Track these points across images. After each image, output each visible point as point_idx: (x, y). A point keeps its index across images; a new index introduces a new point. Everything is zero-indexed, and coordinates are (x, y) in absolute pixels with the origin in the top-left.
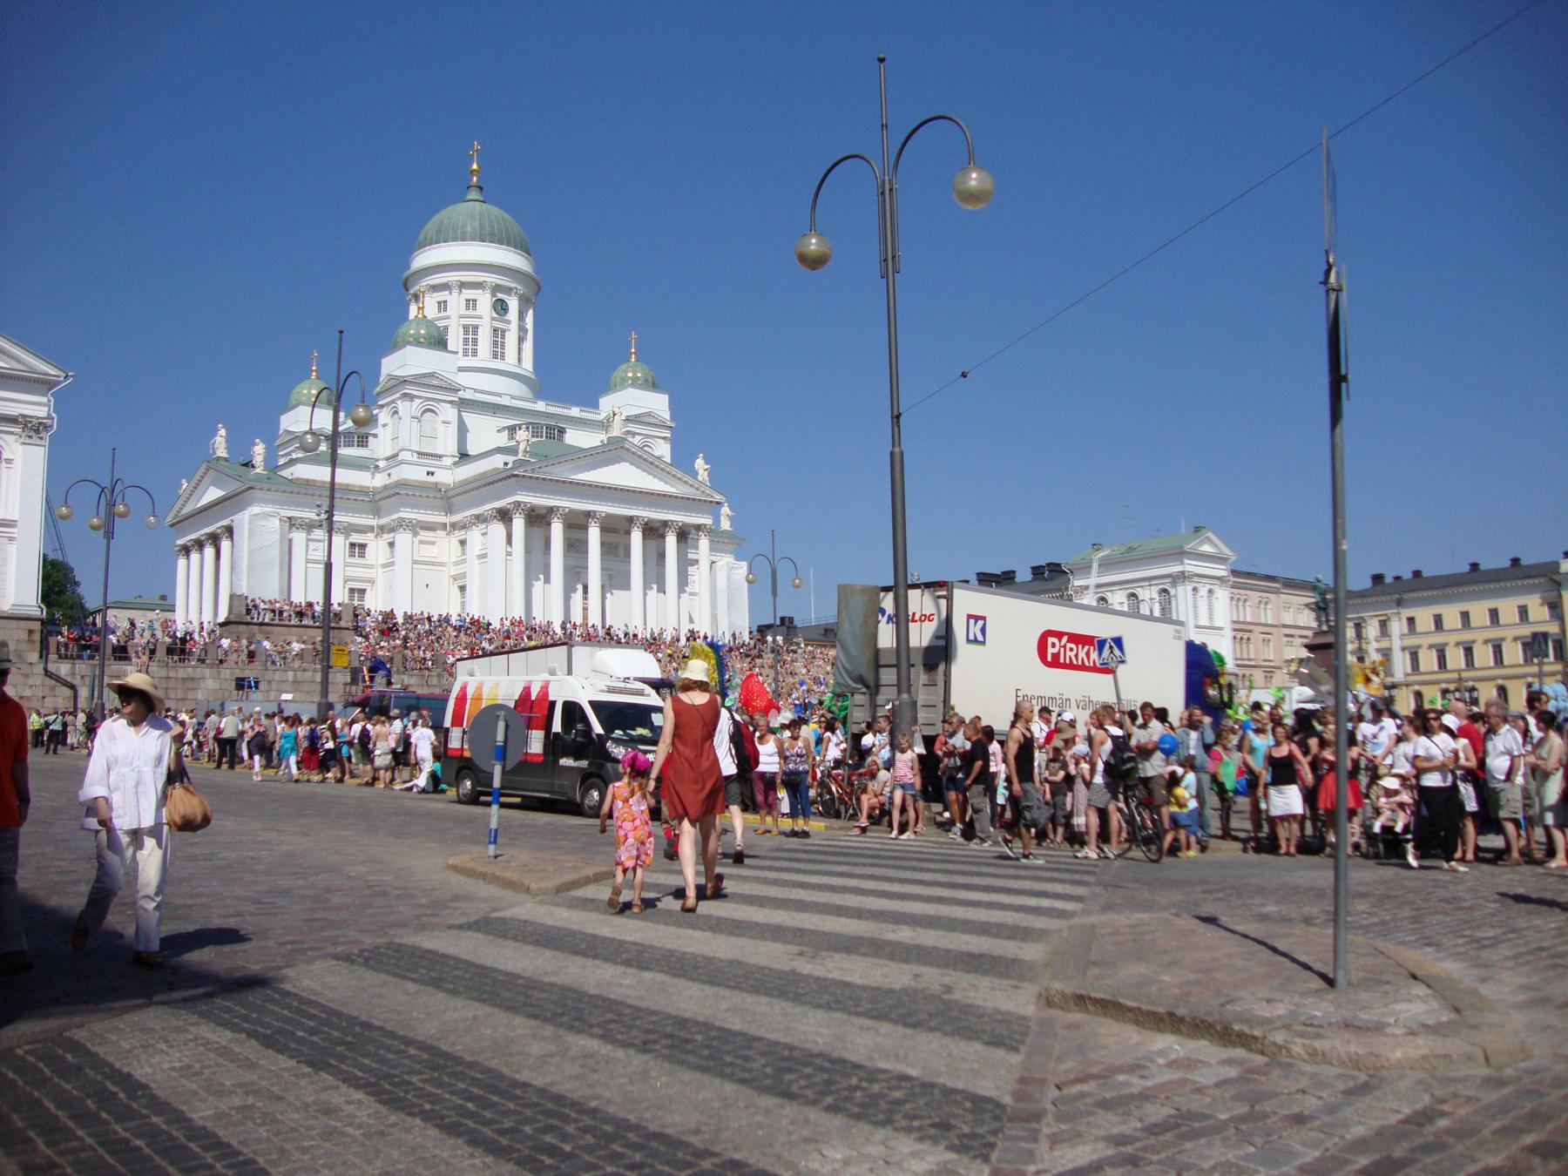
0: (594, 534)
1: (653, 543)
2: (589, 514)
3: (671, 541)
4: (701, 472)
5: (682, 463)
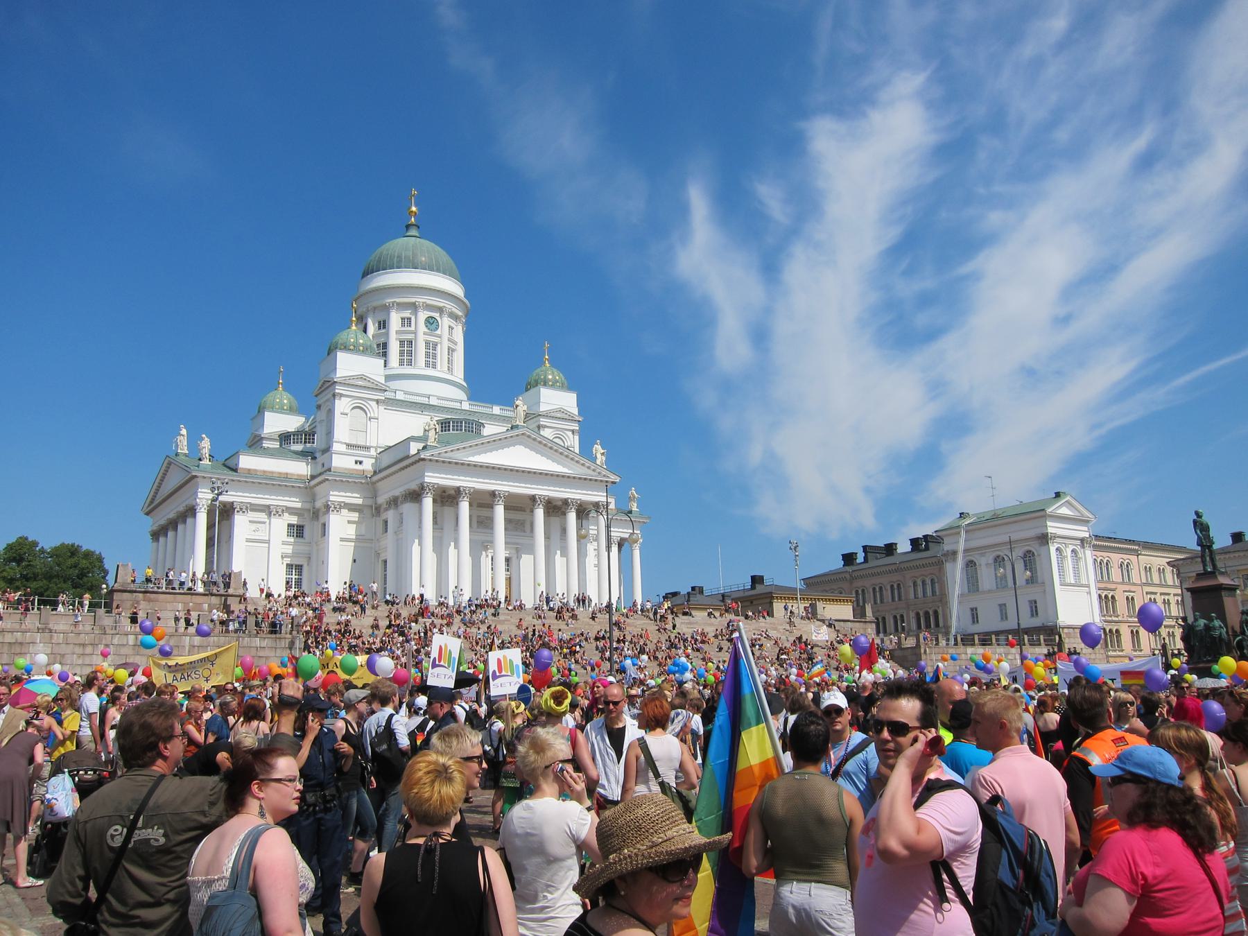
0: (500, 511)
1: (555, 521)
2: (493, 494)
3: (572, 517)
4: (599, 456)
5: (586, 451)
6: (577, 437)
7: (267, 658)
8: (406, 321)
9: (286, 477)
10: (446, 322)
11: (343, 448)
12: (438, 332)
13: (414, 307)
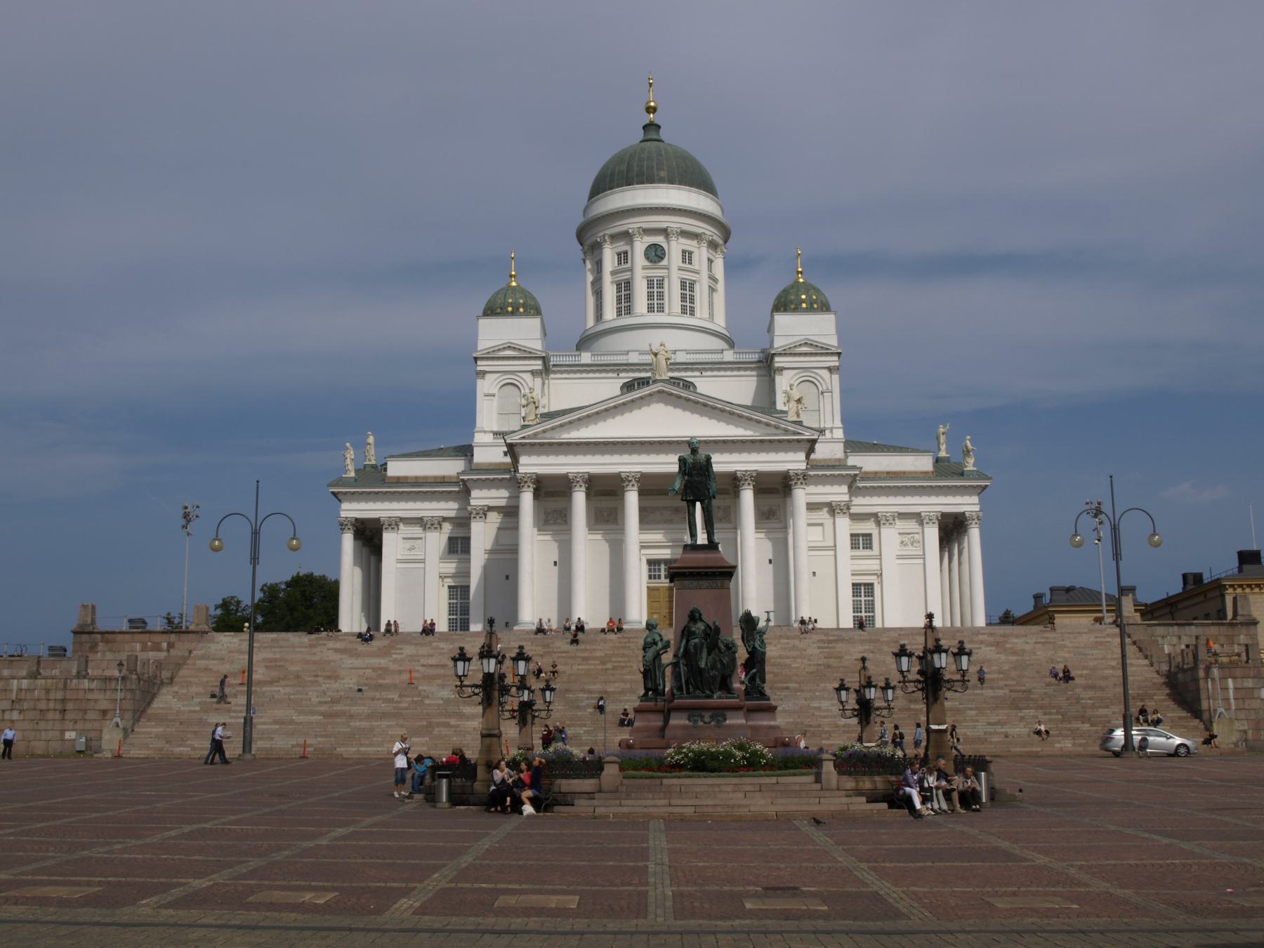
6: (836, 377)
7: (96, 701)
8: (623, 257)
9: (442, 481)
10: (675, 248)
11: (489, 438)
12: (664, 262)
13: (627, 236)
